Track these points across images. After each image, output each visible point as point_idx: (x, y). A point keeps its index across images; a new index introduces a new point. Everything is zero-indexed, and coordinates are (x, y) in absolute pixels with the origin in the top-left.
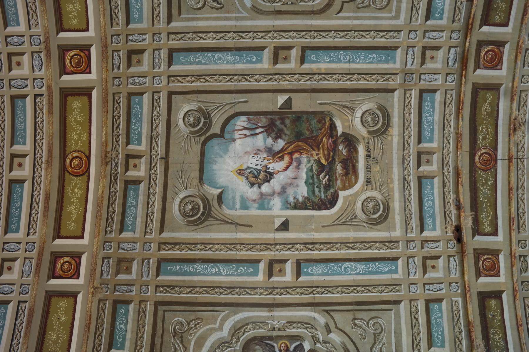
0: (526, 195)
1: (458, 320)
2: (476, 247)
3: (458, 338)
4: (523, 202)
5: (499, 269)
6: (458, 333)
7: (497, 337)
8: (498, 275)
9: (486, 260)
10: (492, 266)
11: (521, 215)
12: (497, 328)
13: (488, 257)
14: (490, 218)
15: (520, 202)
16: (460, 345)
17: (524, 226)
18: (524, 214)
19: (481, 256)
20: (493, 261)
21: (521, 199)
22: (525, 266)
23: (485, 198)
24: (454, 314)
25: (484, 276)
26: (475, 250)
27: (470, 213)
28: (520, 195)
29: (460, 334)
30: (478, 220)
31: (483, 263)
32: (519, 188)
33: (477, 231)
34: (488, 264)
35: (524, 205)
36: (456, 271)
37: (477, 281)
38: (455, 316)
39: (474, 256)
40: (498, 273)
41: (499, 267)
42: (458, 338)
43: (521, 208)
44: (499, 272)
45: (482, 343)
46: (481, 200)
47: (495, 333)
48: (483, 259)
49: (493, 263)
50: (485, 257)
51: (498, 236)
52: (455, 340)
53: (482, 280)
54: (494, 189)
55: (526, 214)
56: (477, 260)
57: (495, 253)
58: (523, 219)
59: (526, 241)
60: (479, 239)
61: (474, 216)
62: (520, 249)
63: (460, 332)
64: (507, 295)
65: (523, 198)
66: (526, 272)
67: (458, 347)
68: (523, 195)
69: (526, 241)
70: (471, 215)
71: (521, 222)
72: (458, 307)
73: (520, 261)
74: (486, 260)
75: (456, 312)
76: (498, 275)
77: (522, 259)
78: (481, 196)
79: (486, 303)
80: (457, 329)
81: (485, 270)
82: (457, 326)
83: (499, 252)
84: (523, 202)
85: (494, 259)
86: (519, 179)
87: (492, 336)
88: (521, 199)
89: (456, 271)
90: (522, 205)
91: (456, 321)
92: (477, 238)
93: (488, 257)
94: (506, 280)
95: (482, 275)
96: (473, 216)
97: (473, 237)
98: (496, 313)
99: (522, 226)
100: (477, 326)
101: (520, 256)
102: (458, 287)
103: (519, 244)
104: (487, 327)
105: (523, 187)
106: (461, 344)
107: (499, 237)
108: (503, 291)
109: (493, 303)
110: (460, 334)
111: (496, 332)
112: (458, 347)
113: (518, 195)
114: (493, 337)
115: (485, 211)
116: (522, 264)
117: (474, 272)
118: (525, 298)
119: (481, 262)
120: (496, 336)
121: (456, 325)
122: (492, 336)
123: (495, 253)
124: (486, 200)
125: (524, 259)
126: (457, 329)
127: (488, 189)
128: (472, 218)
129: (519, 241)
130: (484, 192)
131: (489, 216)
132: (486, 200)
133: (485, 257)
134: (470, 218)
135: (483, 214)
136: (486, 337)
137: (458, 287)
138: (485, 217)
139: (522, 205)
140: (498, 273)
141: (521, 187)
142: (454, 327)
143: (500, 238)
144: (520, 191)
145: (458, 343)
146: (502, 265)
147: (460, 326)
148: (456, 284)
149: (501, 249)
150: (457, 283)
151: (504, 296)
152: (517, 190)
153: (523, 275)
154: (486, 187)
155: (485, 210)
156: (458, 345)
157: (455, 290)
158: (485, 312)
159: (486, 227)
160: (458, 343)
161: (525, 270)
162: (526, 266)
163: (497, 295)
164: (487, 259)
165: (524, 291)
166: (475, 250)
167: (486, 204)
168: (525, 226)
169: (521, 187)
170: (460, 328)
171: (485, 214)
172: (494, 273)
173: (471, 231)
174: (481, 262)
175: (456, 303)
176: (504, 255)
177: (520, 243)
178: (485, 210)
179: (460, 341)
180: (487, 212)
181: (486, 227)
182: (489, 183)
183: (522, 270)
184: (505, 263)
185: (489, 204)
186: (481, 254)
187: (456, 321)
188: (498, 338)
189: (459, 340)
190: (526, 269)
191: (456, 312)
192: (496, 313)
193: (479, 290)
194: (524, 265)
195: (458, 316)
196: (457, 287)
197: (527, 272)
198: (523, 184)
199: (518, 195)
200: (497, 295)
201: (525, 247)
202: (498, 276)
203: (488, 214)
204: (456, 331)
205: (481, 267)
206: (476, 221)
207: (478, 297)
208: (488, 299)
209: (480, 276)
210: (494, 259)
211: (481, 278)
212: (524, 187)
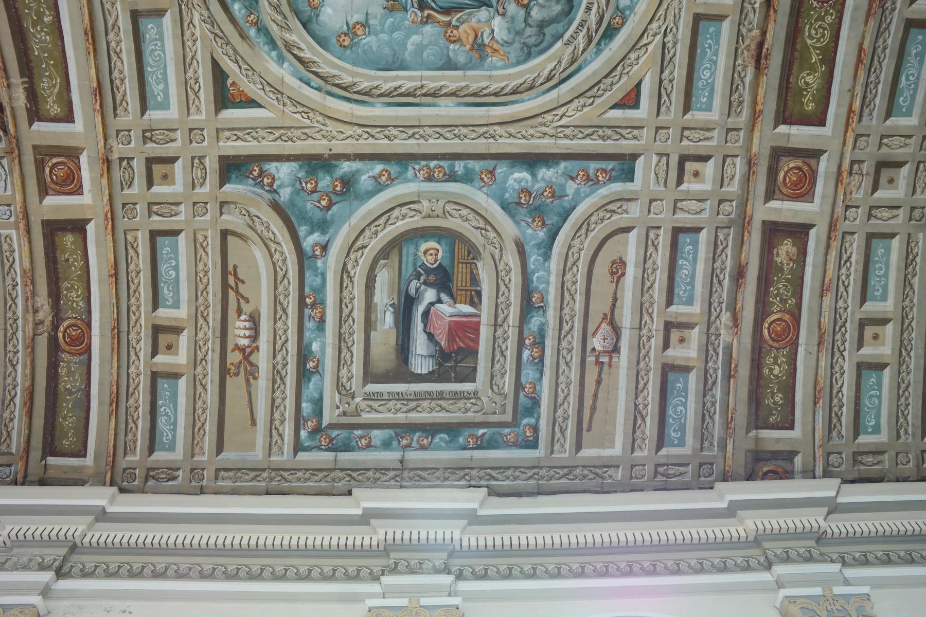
0: (123, 43)
1: (11, 266)
2: (37, 143)
3: (10, 294)
4: (119, 57)
5: (81, 182)
6: (10, 287)
7: (74, 294)
8: (79, 191)
9: (56, 166)
10: (68, 177)
11: (118, 82)
12: (76, 281)
13: (59, 160)
14: (56, 90)
15: (114, 57)
16: (13, 306)
17: (124, 104)
18: (122, 80)
19: (48, 158)
20: (69, 168)
21: (115, 52)
22: (129, 177)
23: (43, 50)
24: (5, 257)
25: (53, 193)
26: (35, 147)
27: (20, 81)
28: (113, 44)
29: (13, 289)
30: (36, 94)
31: (51, 172)
32: (109, 30)
33: (35, 114)
34: (61, 172)
35: (122, 63)
36: (6, 184)
37: (41, 203)
38: (5, 260)
39: (36, 160)
40: (79, 188)
41: (80, 178)
42: (10, 294)
43: (117, 70)
44: (81, 186)
45: (46, 303)
46: (36, 53)
47: (70, 288)
48: (50, 164)
49: (69, 171)
50: (55, 161)
51: (74, 122)
52: (5, 298)
53: (50, 200)
54: (57, 32)
55: (127, 81)
56: (40, 166)
57: (72, 154)
58: (122, 90)
59: (129, 131)
60: (41, 129)
61: (26, 85)
62: (121, 146)
63: (14, 286)
64: (97, 226)
65: (118, 50)
66: (130, 186)
67: (10, 309)
68: (118, 43)
69: (129, 131)
70: (23, 83)
71: (119, 97)
72: (10, 245)
73: (120, 167)
74: (56, 166)
75: (8, 254)
76: (79, 191)
77: (125, 163)
78: (36, 47)
79: (56, 239)
80: (9, 281)
81: (56, 183)
82: (10, 277)
83: (79, 152)
84: (119, 57)
85: (71, 165)
86: (107, 12)
87: (65, 292)
88: (115, 52)
89: (6, 184)
90: (119, 64)
91: (7, 267)
92: (38, 126)
93: (59, 160)
94: (93, 201)
95: (50, 192)
96: (26, 85)
97: (31, 125)
98: (75, 256)
99: (121, 104)
100: (40, 276)
101: (121, 159)
102: (11, 212)
103: (117, 136)
104: (57, 279)
105: (116, 27)
106: (15, 304)
107: (76, 125)
108: (89, 220)
109: (69, 239)
110: (13, 289)
111: (72, 286)
112: (10, 309)
113: (108, 44)
114: (68, 293)
115: (47, 76)
116: (124, 172)
117: (36, 188)
118: (128, 232)
119: (47, 170)
120: (72, 292)
121: (8, 274)
122: (65, 292)
123: (72, 154)
124: (46, 55)
125: (128, 163)
126: (9, 281)
127: (45, 32)
128: (25, 89)
129: (118, 132)
130: (39, 40)
131: (54, 86)
132: (46, 55)
133: (55, 161)
134: (21, 90)
135: (43, 82)
136: (55, 294)
137: (11, 212)
138: (48, 86)
139: (119, 64)
140: (79, 188)
141: (113, 28)
142: (4, 278)
143: (78, 126)
144: (111, 36)
145: (10, 302)
146: (86, 175)
147: (14, 277)
148: (7, 208)
149: (82, 145)
150: (9, 205)
151: (91, 228)
152: (107, 34)
153: (126, 191)
154: (42, 30)
155: (47, 74)
156: (10, 306)
157: (6, 217)
158: (55, 254)
159: (51, 107)
160: (10, 302)
161: (129, 183)
162: (132, 176)
163: (78, 227)
164: (58, 163)
165: (126, 219)
166: (35, 147)
167: (46, 62)
168: (127, 104)
169: (113, 28)
170: (14, 280)
171: (48, 82)
172: (72, 188)
173: (25, 113)
174: (47, 170)
175: (8, 239)
176: (89, 157)
177: (120, 136)
178: (47, 74)
179: (13, 300)
180: (50, 77)
181: (51, 107)
182: (46, 19)
183: (124, 183)
184: (91, 171)
185: (52, 62)
186: (46, 155)
187: (7, 267)
188: (75, 296)
189: (12, 298)
190: (131, 183)
191: (8, 254)
192: (75, 256)
193: (46, 218)
194: (127, 175)
195: (11, 259)
196: (8, 213)
197: (132, 187)
198: (116, 21)
199: (108, 44)
200: (78, 227)
201: (129, 143)
202: (79, 194)
203: (52, 81)
204: (7, 284)
205: (49, 178)
206: (32, 95)
207: (43, 229)
208: (59, 233)
209: (47, 194)
210: (71, 165)
211: (48, 198)
212: (119, 29)
